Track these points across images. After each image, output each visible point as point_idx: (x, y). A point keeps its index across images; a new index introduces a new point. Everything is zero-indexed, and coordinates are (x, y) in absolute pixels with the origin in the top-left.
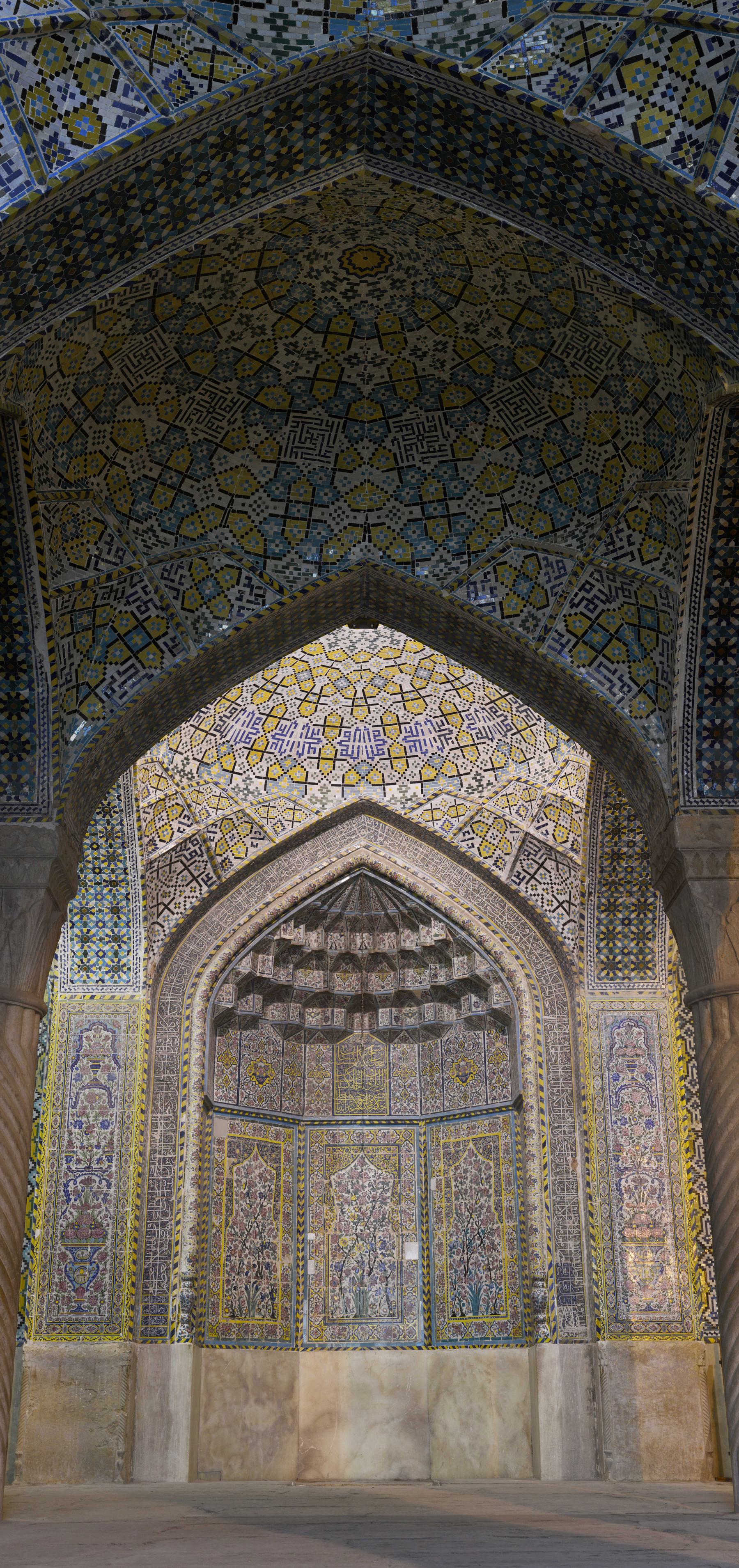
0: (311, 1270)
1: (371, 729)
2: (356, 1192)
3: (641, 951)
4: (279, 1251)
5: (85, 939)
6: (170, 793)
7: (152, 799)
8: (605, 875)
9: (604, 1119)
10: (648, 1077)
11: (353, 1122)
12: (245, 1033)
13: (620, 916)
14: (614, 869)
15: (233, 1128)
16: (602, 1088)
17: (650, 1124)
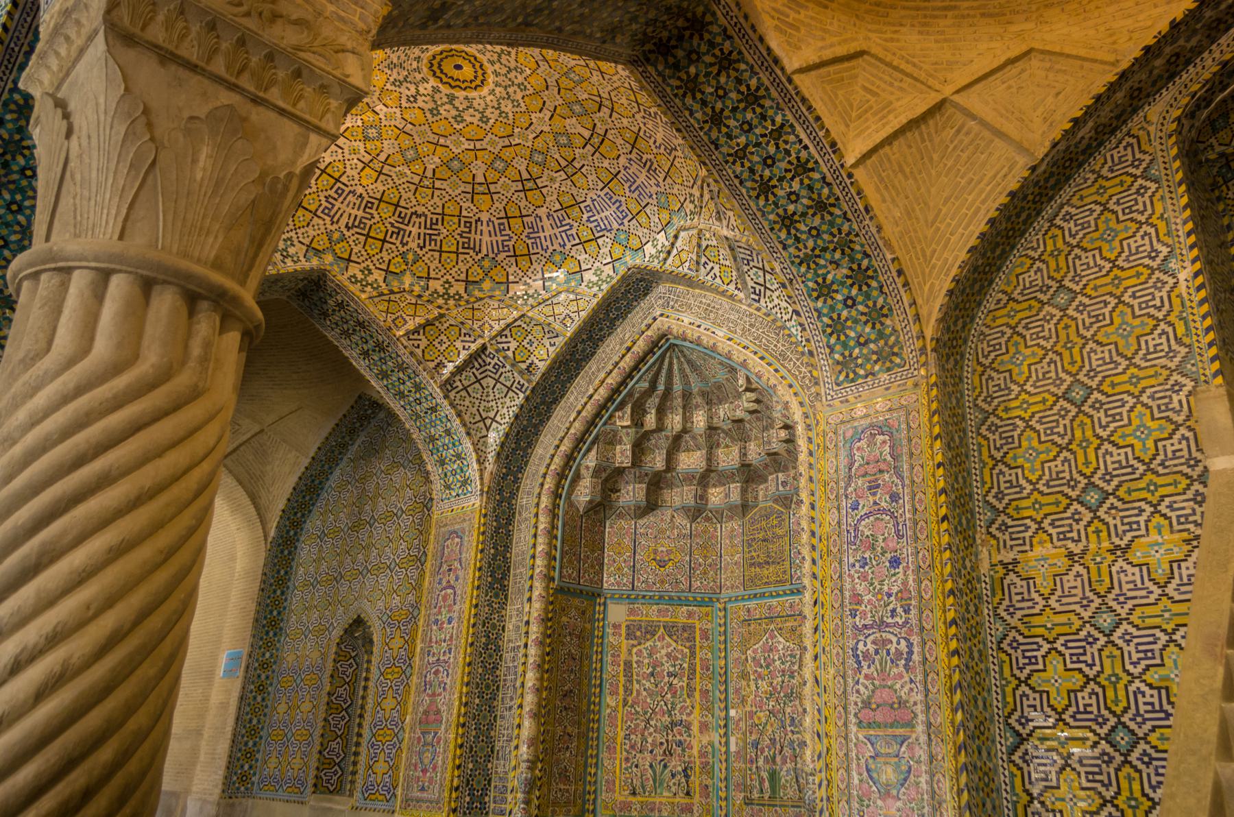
0: (733, 748)
1: (602, 194)
2: (767, 667)
3: (881, 335)
4: (695, 728)
5: (442, 462)
6: (431, 317)
7: (411, 325)
8: (792, 250)
9: (840, 563)
10: (894, 497)
11: (763, 595)
12: (641, 522)
13: (839, 297)
14: (797, 239)
15: (632, 612)
16: (839, 523)
17: (895, 562)
